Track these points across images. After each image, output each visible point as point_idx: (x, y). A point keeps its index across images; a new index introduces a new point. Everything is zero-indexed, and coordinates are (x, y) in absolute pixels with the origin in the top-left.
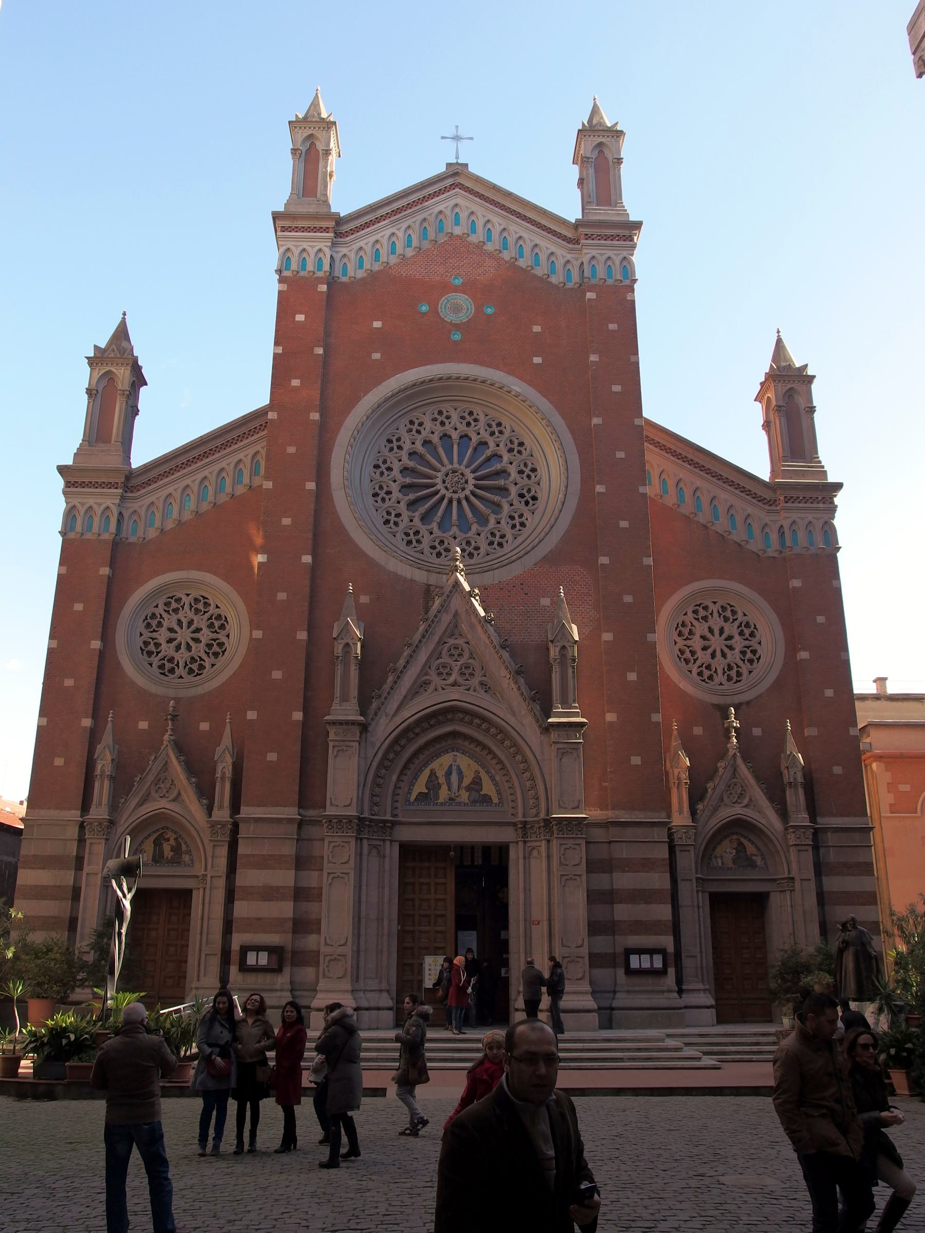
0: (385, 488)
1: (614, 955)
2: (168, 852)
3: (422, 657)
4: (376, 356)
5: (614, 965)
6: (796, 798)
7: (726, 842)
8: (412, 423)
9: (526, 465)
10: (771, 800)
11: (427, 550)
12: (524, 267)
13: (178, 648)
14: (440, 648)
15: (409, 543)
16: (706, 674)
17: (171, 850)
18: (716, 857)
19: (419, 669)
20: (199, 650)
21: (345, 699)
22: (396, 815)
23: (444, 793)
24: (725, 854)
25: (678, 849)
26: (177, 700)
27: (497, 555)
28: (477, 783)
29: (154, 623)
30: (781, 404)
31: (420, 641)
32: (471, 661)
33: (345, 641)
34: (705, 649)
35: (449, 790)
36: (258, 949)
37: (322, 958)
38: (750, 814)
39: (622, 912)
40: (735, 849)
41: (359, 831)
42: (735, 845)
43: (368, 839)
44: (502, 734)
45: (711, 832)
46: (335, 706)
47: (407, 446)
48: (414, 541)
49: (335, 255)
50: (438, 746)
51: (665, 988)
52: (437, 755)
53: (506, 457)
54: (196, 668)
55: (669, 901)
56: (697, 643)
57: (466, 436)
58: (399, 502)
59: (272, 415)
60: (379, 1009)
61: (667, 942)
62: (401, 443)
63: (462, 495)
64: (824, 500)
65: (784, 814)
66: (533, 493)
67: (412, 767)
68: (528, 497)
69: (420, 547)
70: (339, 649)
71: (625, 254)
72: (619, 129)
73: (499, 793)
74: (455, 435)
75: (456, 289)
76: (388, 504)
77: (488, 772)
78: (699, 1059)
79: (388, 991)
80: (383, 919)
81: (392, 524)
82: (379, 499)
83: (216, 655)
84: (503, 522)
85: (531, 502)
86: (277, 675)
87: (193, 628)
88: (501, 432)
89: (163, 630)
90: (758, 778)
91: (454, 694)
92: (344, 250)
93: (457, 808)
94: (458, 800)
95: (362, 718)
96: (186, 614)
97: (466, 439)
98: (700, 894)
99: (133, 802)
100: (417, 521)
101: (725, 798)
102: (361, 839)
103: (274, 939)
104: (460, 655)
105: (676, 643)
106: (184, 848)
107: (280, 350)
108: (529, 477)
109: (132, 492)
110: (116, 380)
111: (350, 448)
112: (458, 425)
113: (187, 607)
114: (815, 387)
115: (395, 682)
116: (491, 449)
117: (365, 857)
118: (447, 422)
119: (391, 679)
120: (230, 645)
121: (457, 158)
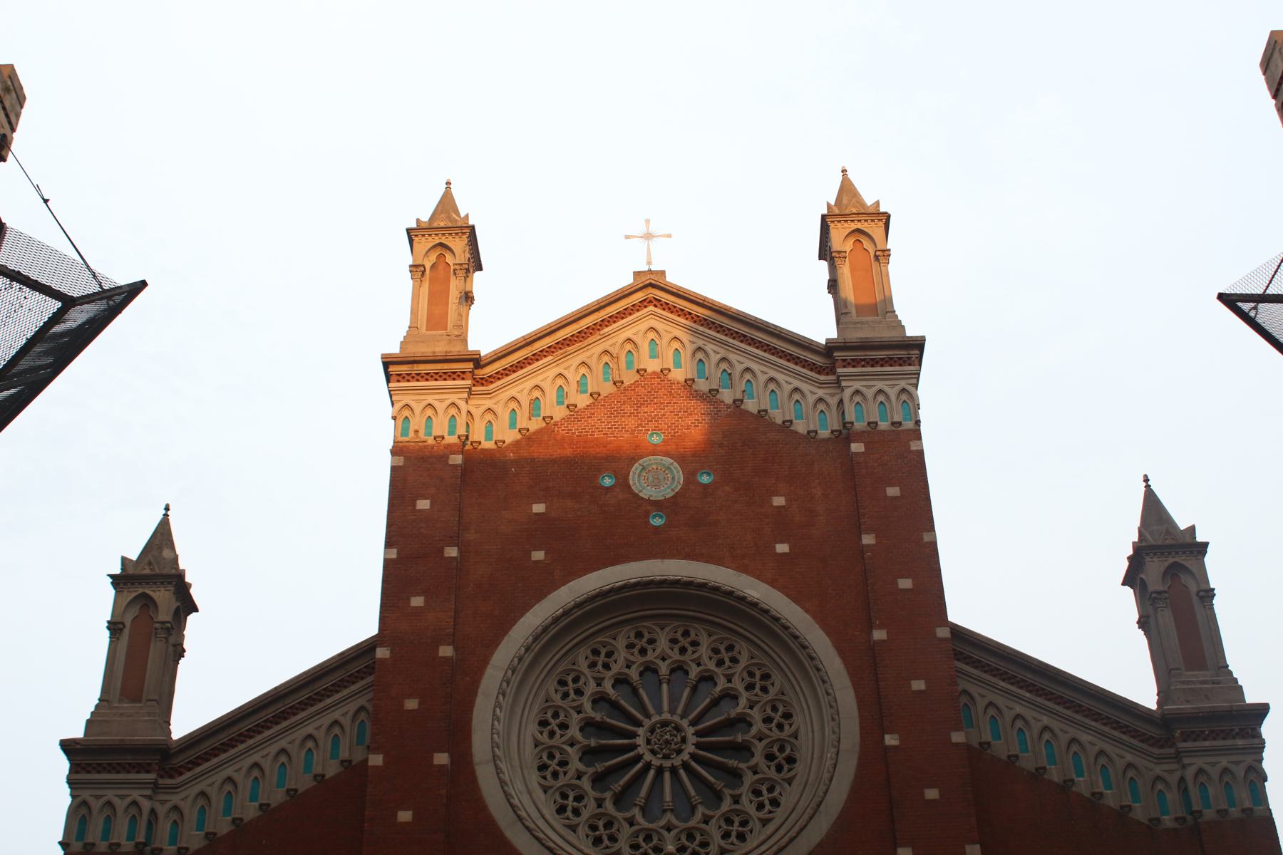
0: (558, 756)
4: (538, 555)
8: (596, 652)
9: (775, 709)
12: (755, 411)
30: (1161, 588)
47: (591, 688)
48: (605, 838)
49: (473, 410)
59: (382, 653)
63: (677, 761)
64: (1243, 734)
66: (788, 751)
68: (780, 757)
71: (903, 384)
72: (882, 210)
74: (664, 668)
76: (562, 780)
81: (569, 813)
84: (744, 800)
92: (488, 403)
97: (680, 673)
100: (609, 806)
107: (393, 554)
108: (780, 727)
109: (171, 777)
111: (501, 697)
112: (669, 651)
114: (1209, 560)
116: (718, 689)
118: (649, 648)
121: (649, 263)
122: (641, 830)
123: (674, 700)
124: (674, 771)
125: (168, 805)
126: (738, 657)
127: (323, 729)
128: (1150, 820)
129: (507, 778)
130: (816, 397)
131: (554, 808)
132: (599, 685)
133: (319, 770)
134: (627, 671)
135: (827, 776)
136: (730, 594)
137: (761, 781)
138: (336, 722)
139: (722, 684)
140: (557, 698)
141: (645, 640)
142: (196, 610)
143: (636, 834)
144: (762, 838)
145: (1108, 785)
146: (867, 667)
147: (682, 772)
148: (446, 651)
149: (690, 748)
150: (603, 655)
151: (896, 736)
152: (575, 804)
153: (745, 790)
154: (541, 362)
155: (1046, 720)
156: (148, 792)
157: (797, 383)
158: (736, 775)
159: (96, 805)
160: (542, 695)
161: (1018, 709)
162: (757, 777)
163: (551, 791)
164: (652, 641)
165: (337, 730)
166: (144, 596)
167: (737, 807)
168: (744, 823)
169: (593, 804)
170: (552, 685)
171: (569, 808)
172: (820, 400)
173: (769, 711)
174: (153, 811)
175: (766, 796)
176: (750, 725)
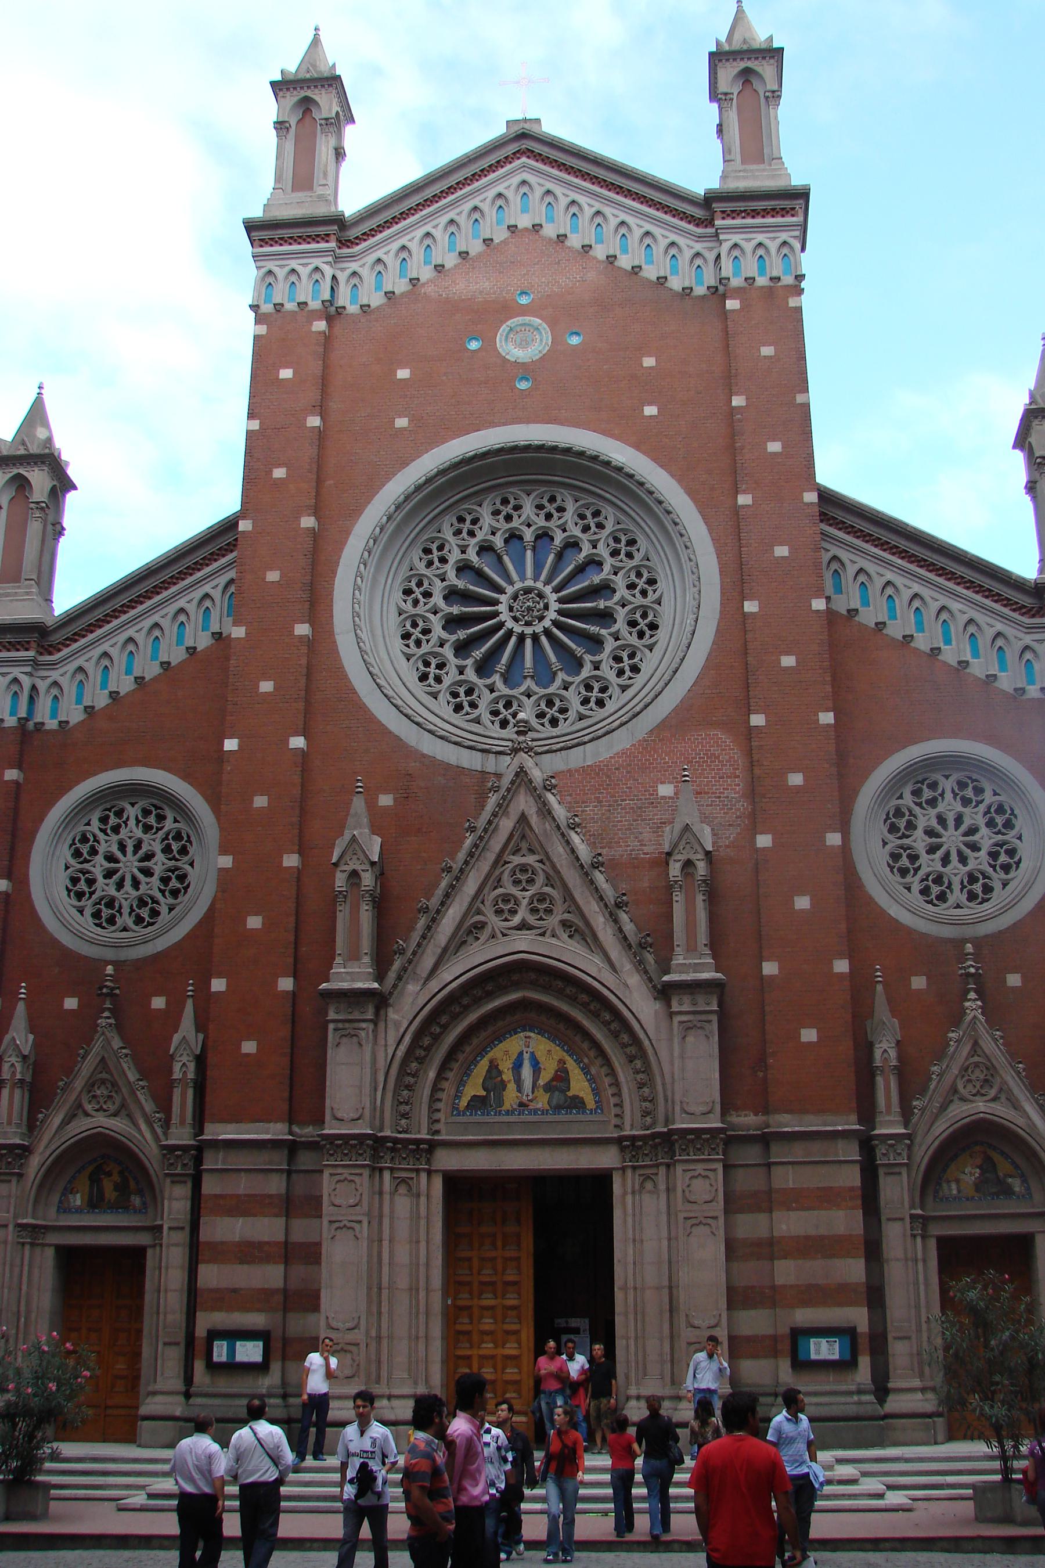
0: (421, 624)
1: (774, 1338)
2: (110, 1193)
3: (471, 886)
5: (775, 1354)
8: (461, 520)
9: (639, 575)
11: (486, 718)
13: (120, 885)
14: (497, 873)
15: (458, 708)
16: (935, 889)
18: (949, 1182)
19: (466, 905)
20: (151, 886)
21: (354, 956)
22: (437, 1132)
24: (962, 1176)
25: (881, 1172)
26: (117, 964)
28: (561, 1077)
29: (85, 850)
31: (466, 863)
32: (547, 889)
34: (932, 850)
35: (519, 1089)
39: (787, 1272)
40: (980, 1167)
41: (376, 1157)
42: (979, 1161)
43: (392, 1169)
45: (937, 1143)
48: (466, 704)
50: (500, 1023)
51: (853, 1388)
52: (500, 1038)
53: (609, 562)
54: (147, 912)
55: (862, 1252)
56: (919, 841)
61: (859, 1317)
63: (539, 628)
66: (650, 618)
67: (461, 1057)
68: (643, 624)
69: (477, 712)
70: (340, 881)
73: (596, 1092)
74: (528, 535)
75: (524, 311)
76: (425, 648)
77: (578, 1061)
78: (880, 1496)
80: (417, 1290)
81: (431, 681)
83: (175, 893)
84: (604, 666)
85: (648, 633)
86: (254, 922)
87: (141, 853)
89: (99, 859)
90: (1013, 1056)
91: (523, 944)
92: (354, 266)
95: (376, 985)
96: (132, 831)
97: (546, 539)
98: (919, 1240)
99: (57, 1121)
100: (471, 675)
101: (960, 1087)
102: (381, 1170)
103: (256, 1320)
104: (531, 881)
105: (885, 844)
106: (132, 1184)
107: (255, 425)
108: (644, 593)
109: (50, 654)
111: (362, 566)
112: (534, 518)
113: (132, 822)
116: (583, 554)
117: (387, 1197)
118: (515, 514)
120: (193, 875)
123: (538, 566)
124: (535, 637)
125: (49, 681)
126: (605, 522)
127: (195, 602)
128: (1016, 690)
129: (368, 648)
130: (693, 251)
131: (416, 676)
132: (463, 552)
134: (491, 538)
135: (685, 642)
136: (595, 458)
137: (622, 648)
138: (207, 596)
139: (586, 550)
140: (421, 568)
141: (510, 506)
142: (75, 488)
143: (496, 701)
144: (620, 705)
145: (976, 654)
146: (733, 533)
147: (543, 639)
150: (468, 522)
151: (756, 603)
153: (605, 656)
154: (408, 221)
155: (916, 588)
156: (28, 669)
157: (673, 237)
158: (597, 642)
163: (412, 660)
164: (517, 508)
165: (208, 603)
166: (19, 477)
167: (597, 673)
168: (603, 690)
169: (453, 671)
170: (416, 553)
171: (431, 676)
172: (698, 254)
173: (633, 577)
174: (34, 688)
175: (626, 663)
176: (614, 591)
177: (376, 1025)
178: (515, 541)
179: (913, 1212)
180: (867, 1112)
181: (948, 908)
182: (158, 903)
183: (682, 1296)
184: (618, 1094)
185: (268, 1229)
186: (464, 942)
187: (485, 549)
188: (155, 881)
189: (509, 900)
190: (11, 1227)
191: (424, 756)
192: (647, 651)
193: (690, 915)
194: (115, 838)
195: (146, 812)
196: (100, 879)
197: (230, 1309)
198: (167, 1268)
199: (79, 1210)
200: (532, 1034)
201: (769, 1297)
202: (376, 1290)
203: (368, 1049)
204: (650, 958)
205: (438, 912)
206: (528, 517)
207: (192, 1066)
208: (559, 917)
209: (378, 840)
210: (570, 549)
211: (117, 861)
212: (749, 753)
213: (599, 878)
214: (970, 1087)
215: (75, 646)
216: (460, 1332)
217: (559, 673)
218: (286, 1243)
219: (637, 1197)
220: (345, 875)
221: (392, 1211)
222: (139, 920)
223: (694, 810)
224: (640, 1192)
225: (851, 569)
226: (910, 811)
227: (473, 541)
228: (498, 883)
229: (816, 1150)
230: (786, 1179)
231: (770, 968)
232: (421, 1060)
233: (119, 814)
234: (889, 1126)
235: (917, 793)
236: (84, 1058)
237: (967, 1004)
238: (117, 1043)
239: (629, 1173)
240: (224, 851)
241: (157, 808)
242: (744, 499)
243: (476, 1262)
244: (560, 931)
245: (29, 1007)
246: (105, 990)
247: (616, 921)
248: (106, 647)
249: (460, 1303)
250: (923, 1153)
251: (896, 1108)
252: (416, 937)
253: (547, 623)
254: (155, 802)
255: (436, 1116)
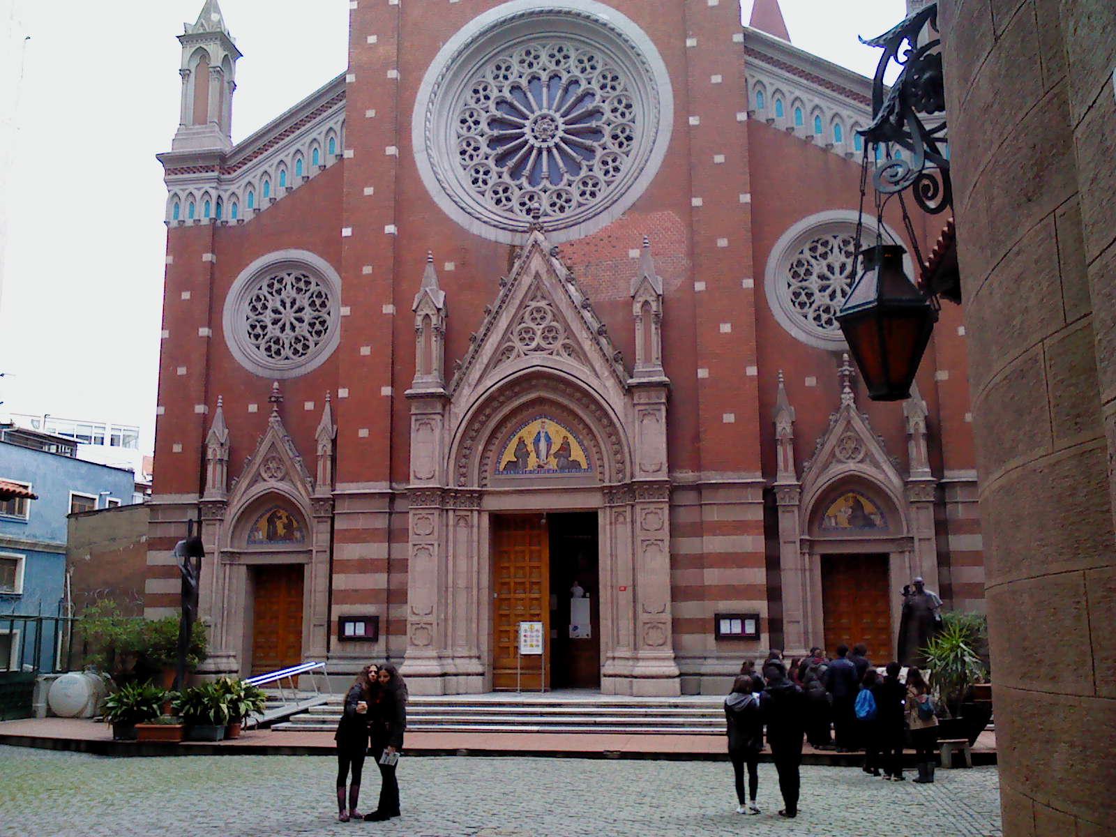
2: (281, 531)
5: (704, 631)
6: (919, 450)
7: (841, 501)
8: (499, 68)
9: (620, 102)
10: (888, 452)
11: (517, 207)
13: (283, 329)
14: (521, 313)
15: (498, 202)
17: (284, 528)
18: (830, 518)
20: (303, 329)
21: (428, 372)
23: (532, 461)
24: (838, 514)
25: (780, 510)
27: (586, 207)
28: (565, 448)
29: (259, 306)
31: (500, 307)
32: (554, 324)
33: (423, 313)
36: (355, 619)
37: (409, 626)
38: (867, 470)
39: (712, 576)
40: (851, 507)
41: (443, 501)
42: (851, 503)
43: (454, 510)
44: (586, 397)
46: (418, 378)
47: (494, 94)
48: (503, 199)
52: (526, 424)
53: (599, 93)
54: (299, 348)
57: (556, 76)
58: (487, 158)
60: (468, 675)
62: (488, 92)
63: (551, 143)
65: (903, 468)
66: (627, 132)
67: (500, 436)
68: (622, 137)
69: (510, 204)
74: (544, 76)
76: (476, 160)
79: (479, 658)
81: (480, 183)
82: (467, 157)
83: (319, 333)
84: (595, 168)
85: (626, 143)
87: (296, 307)
88: (593, 68)
89: (268, 312)
91: (537, 360)
93: (547, 475)
94: (546, 467)
95: (442, 390)
96: (289, 293)
98: (807, 556)
100: (506, 178)
101: (837, 453)
103: (369, 609)
104: (543, 318)
105: (789, 285)
107: (355, 5)
108: (623, 115)
110: (210, 56)
111: (430, 104)
112: (547, 64)
113: (289, 287)
115: (476, 351)
116: (582, 88)
117: (451, 528)
118: (535, 62)
119: (472, 348)
122: (528, 192)
123: (551, 99)
125: (229, 193)
132: (500, 91)
133: (322, 163)
135: (649, 149)
137: (608, 155)
138: (331, 129)
140: (472, 104)
141: (532, 56)
144: (606, 194)
146: (683, 68)
147: (555, 151)
148: (393, 74)
149: (560, 133)
151: (697, 118)
152: (484, 177)
153: (596, 162)
155: (817, 101)
156: (215, 185)
159: (183, 195)
160: (461, 103)
161: (797, 93)
162: (605, 151)
164: (536, 57)
165: (332, 134)
167: (591, 173)
168: (595, 185)
171: (480, 180)
176: (603, 114)
177: (443, 416)
178: (536, 81)
179: (802, 537)
180: (769, 468)
181: (833, 330)
182: (308, 340)
183: (640, 591)
184: (601, 459)
185: (377, 550)
186: (501, 360)
187: (515, 88)
188: (305, 325)
189: (529, 332)
190: (216, 554)
191: (474, 235)
192: (624, 156)
193: (647, 340)
194: (278, 298)
195: (298, 280)
196: (270, 325)
197: (353, 603)
198: (315, 578)
199: (261, 542)
200: (547, 420)
201: (700, 593)
202: (443, 589)
203: (437, 432)
204: (620, 368)
205: (482, 340)
206: (544, 63)
207: (329, 446)
208: (561, 343)
209: (442, 294)
210: (572, 86)
211: (280, 313)
212: (690, 225)
213: (587, 315)
214: (844, 451)
215: (245, 167)
216: (502, 615)
217: (565, 175)
218: (389, 559)
219: (613, 526)
220: (422, 317)
221: (455, 537)
222: (296, 352)
223: (652, 267)
224: (616, 524)
225: (770, 90)
226: (808, 262)
227: (507, 83)
228: (522, 321)
229: (733, 495)
230: (713, 515)
231: (703, 373)
232: (473, 439)
233: (280, 281)
234: (786, 478)
235: (813, 249)
236: (261, 444)
237: (843, 396)
238: (282, 433)
239: (608, 510)
240: (345, 304)
241: (304, 276)
242: (691, 42)
243: (512, 570)
244: (562, 351)
245: (224, 412)
246: (273, 399)
247: (598, 344)
248: (265, 167)
249: (503, 596)
250: (810, 499)
251: (791, 467)
252: (468, 357)
253: (557, 139)
254: (305, 273)
255: (485, 475)
